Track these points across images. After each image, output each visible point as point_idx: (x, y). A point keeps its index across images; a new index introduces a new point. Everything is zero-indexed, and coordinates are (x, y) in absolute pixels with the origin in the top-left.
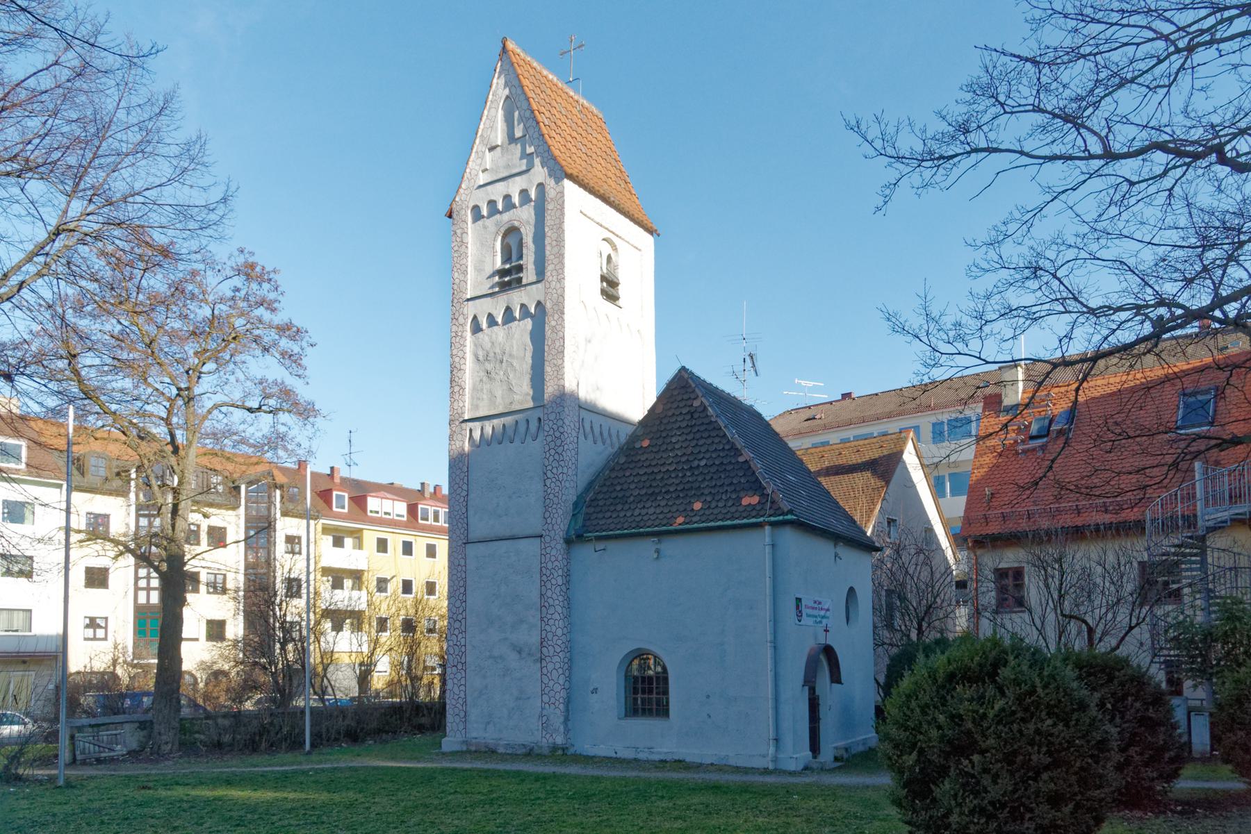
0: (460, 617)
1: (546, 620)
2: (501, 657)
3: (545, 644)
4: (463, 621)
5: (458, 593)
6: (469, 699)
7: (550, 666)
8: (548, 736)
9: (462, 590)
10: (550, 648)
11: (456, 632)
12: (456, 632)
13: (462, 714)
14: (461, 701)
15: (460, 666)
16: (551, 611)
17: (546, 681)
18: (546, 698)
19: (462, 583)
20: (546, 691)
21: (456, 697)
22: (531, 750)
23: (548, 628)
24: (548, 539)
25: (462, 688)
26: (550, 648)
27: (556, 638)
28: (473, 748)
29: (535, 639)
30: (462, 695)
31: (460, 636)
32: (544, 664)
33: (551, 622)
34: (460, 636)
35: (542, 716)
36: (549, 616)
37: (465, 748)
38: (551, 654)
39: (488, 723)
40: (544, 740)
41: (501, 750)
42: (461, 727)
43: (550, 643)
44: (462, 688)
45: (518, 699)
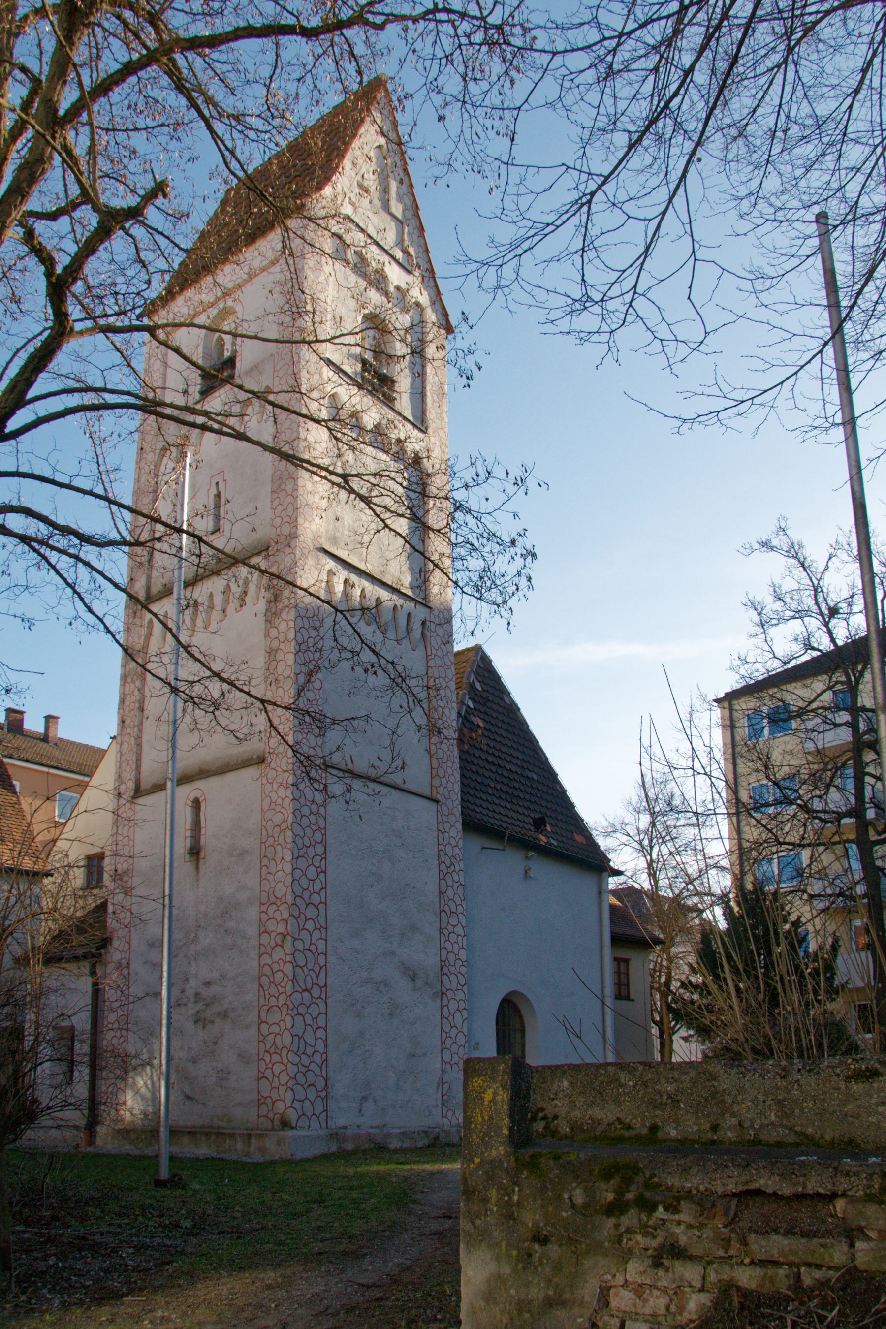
0: (316, 899)
1: (445, 932)
2: (386, 983)
3: (445, 970)
4: (322, 907)
5: (311, 853)
6: (333, 1057)
7: (453, 1005)
8: (450, 1114)
9: (320, 849)
10: (452, 977)
11: (310, 925)
12: (310, 925)
13: (321, 1084)
14: (317, 1058)
15: (316, 992)
16: (453, 921)
17: (447, 1029)
18: (447, 1057)
19: (318, 836)
20: (448, 1042)
21: (310, 1050)
22: (437, 1138)
23: (448, 945)
24: (444, 808)
25: (320, 1033)
26: (452, 977)
27: (459, 963)
28: (349, 1147)
29: (429, 960)
30: (320, 1046)
31: (317, 934)
32: (445, 1002)
33: (453, 937)
34: (317, 934)
35: (442, 1083)
36: (450, 929)
37: (334, 1148)
38: (454, 986)
39: (365, 1098)
40: (446, 1121)
41: (394, 1144)
42: (319, 1109)
43: (452, 969)
44: (320, 1033)
45: (411, 1056)
